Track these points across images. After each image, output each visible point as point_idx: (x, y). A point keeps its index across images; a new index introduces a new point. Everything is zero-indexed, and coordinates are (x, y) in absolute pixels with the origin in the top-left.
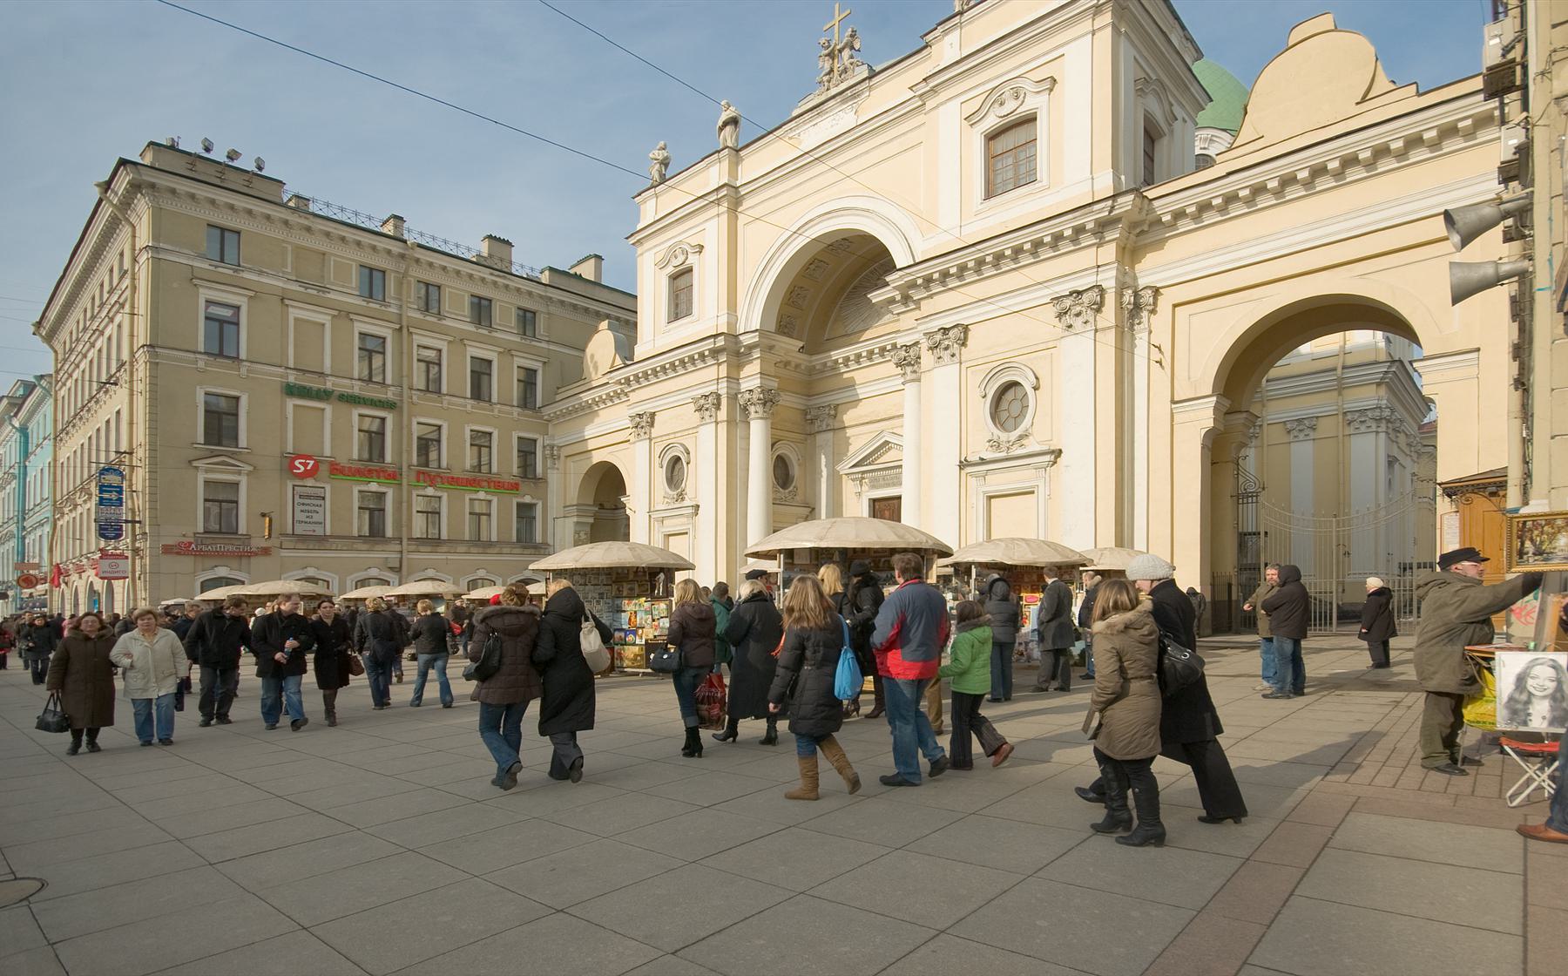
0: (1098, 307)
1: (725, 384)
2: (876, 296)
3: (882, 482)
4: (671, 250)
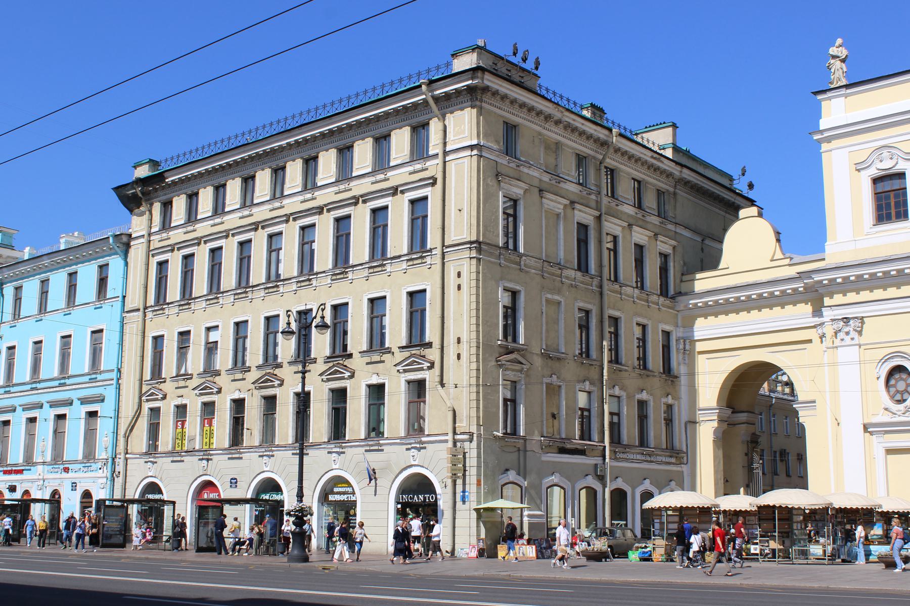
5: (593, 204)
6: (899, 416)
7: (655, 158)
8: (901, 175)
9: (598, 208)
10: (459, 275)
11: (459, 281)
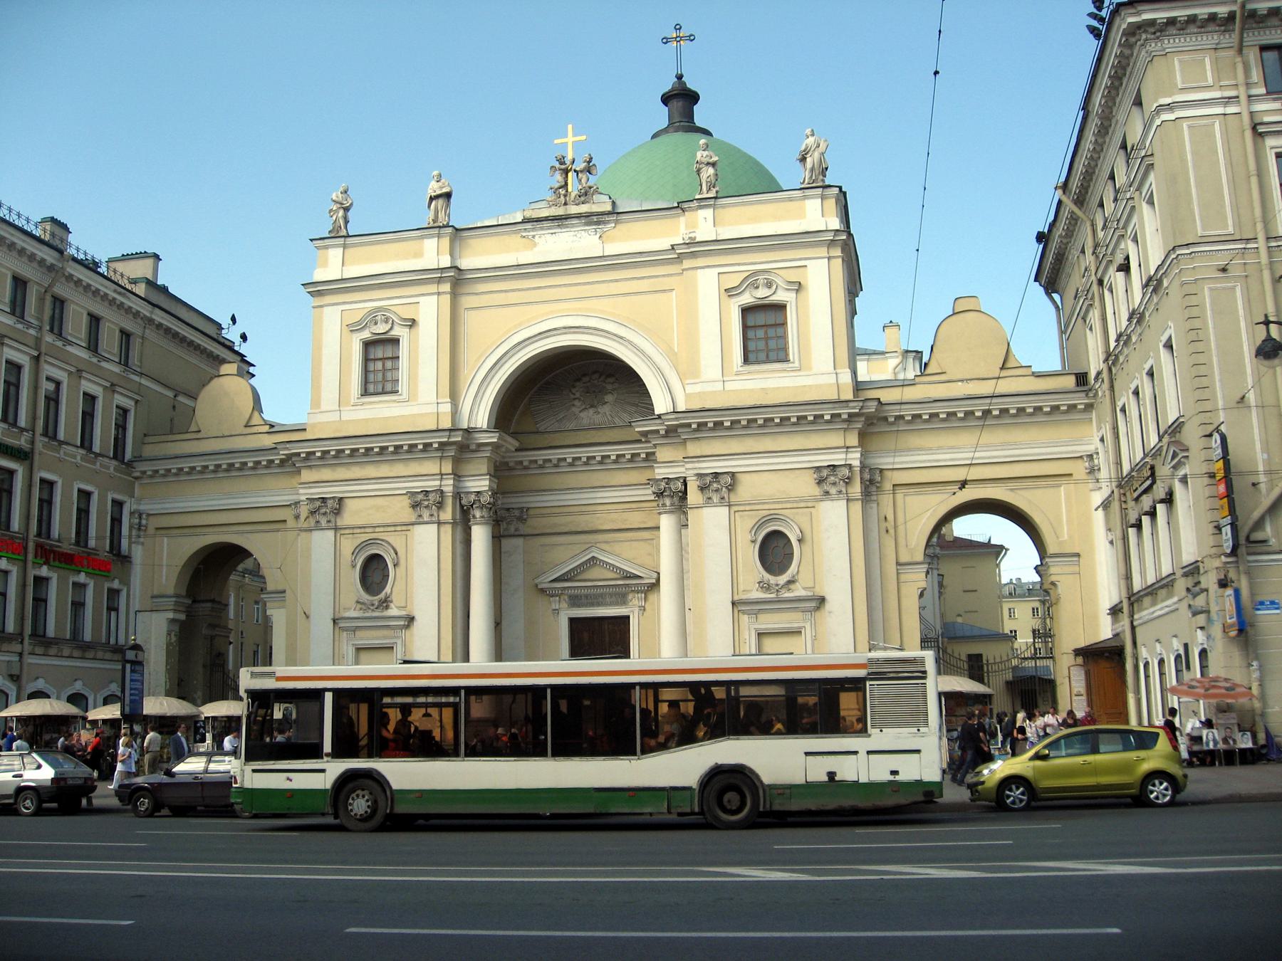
1: (451, 482)
2: (639, 426)
3: (584, 601)
5: (31, 342)
6: (373, 610)
7: (120, 293)
8: (395, 341)
9: (37, 348)
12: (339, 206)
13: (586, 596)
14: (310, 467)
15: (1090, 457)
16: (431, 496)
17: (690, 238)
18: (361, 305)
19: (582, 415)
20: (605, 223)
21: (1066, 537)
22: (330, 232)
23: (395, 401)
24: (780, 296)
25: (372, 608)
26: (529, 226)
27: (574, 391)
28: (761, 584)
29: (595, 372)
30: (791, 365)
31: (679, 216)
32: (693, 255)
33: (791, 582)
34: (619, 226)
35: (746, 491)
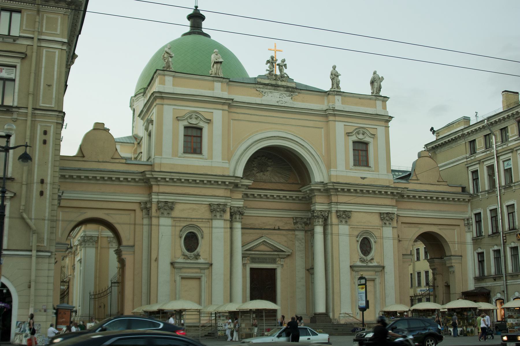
0: (392, 219)
4: (190, 114)
8: (201, 129)
10: (45, 133)
11: (44, 137)
12: (168, 55)
13: (258, 258)
14: (158, 185)
15: (468, 219)
16: (221, 206)
17: (332, 107)
18: (186, 108)
19: (258, 174)
20: (294, 92)
21: (457, 249)
22: (164, 67)
23: (201, 158)
24: (367, 139)
25: (191, 258)
26: (261, 86)
27: (254, 163)
28: (361, 259)
29: (263, 156)
30: (371, 169)
31: (324, 96)
32: (335, 115)
33: (372, 259)
34: (300, 95)
35: (355, 218)
